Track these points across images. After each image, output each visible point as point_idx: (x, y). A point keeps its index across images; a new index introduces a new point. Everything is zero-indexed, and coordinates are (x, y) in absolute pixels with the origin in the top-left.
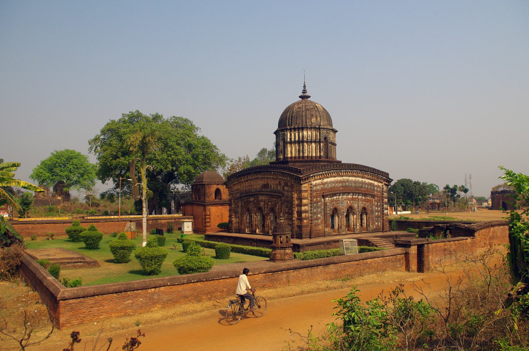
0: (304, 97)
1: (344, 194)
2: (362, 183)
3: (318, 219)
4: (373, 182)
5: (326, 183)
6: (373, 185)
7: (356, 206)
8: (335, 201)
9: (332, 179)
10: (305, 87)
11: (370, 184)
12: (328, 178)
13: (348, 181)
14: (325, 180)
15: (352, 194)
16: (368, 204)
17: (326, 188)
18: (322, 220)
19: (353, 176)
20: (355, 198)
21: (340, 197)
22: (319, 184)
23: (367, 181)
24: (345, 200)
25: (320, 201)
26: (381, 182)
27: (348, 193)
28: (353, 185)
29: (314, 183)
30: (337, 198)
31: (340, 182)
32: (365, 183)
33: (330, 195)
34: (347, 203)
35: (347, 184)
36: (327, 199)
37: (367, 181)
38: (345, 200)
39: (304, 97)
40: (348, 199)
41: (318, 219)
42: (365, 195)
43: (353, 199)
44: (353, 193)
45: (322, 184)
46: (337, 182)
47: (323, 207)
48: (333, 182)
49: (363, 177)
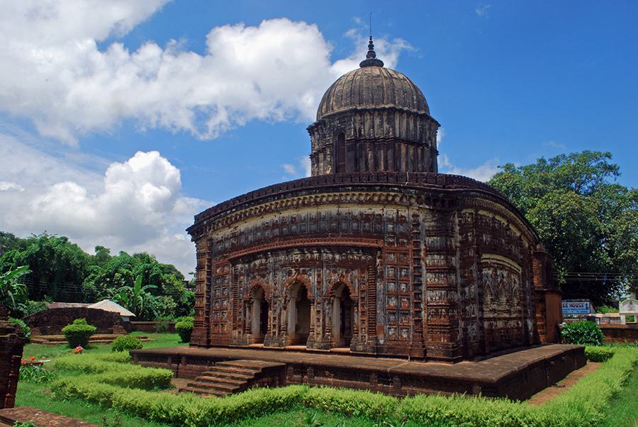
3: (222, 310)
4: (377, 210)
5: (242, 233)
6: (379, 219)
8: (258, 270)
9: (257, 222)
11: (367, 218)
13: (293, 220)
14: (242, 227)
18: (230, 313)
19: (309, 205)
20: (312, 259)
22: (227, 239)
23: (356, 210)
29: (219, 236)
30: (261, 264)
35: (294, 227)
36: (239, 266)
41: (222, 310)
43: (304, 263)
45: (234, 236)
46: (266, 227)
48: (257, 229)
49: (338, 203)
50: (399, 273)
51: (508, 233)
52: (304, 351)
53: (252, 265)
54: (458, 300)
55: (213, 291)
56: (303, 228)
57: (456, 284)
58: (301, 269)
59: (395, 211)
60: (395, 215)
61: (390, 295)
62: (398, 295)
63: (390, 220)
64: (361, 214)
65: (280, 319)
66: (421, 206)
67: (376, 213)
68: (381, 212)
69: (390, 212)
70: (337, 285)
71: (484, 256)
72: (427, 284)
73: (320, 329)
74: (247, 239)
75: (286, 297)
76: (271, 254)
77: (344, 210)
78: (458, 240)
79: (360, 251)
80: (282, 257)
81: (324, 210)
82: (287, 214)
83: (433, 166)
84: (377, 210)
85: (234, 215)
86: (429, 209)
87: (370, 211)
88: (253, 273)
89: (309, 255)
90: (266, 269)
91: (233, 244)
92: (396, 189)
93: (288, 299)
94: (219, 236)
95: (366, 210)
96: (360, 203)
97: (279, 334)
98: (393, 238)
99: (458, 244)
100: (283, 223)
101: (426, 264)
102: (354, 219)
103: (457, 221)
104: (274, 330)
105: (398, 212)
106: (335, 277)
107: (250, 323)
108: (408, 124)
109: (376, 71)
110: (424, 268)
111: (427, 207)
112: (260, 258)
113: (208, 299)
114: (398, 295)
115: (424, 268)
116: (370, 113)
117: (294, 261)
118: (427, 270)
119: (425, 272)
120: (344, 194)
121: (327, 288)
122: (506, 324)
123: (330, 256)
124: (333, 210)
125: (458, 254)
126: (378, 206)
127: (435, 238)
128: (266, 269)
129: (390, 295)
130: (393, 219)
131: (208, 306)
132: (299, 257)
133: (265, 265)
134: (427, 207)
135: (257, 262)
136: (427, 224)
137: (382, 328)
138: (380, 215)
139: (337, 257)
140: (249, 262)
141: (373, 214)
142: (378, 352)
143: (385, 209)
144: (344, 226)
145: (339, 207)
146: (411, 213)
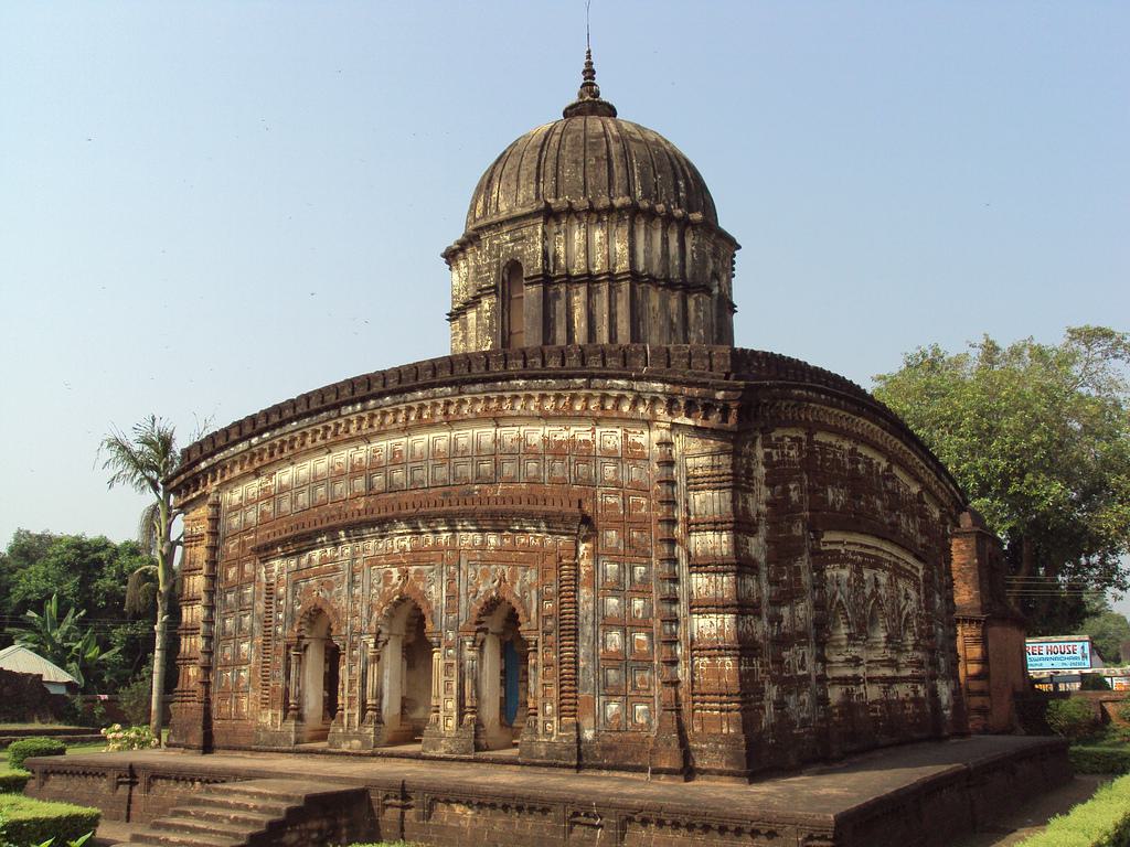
0: (590, 105)
1: (356, 528)
2: (497, 452)
3: (238, 662)
4: (581, 433)
5: (283, 489)
6: (586, 453)
7: (437, 593)
9: (320, 464)
10: (589, 72)
11: (557, 451)
12: (291, 461)
13: (396, 459)
14: (286, 475)
15: (402, 527)
16: (531, 576)
17: (281, 516)
18: (254, 671)
20: (436, 547)
21: (347, 549)
23: (536, 434)
24: (373, 561)
25: (252, 580)
26: (649, 423)
27: (382, 525)
28: (442, 473)
30: (324, 560)
31: (355, 471)
32: (524, 451)
33: (283, 543)
34: (387, 577)
36: (276, 564)
37: (536, 434)
38: (373, 561)
39: (590, 105)
40: (391, 558)
41: (238, 662)
42: (496, 520)
43: (417, 555)
44: (409, 520)
45: (268, 496)
46: (337, 475)
47: (260, 606)
48: (316, 480)
49: (497, 420)
50: (628, 575)
51: (890, 485)
52: (417, 757)
53: (304, 560)
54: (764, 637)
55: (218, 622)
56: (418, 474)
57: (759, 599)
58: (413, 569)
59: (619, 432)
60: (619, 443)
61: (608, 624)
62: (627, 625)
63: (611, 455)
64: (546, 441)
65: (364, 686)
66: (676, 421)
67: (582, 437)
68: (589, 437)
69: (610, 437)
70: (491, 606)
71: (828, 537)
72: (691, 601)
73: (452, 705)
74: (294, 501)
75: (379, 632)
76: (347, 536)
77: (509, 433)
78: (763, 497)
79: (543, 525)
80: (372, 545)
81: (465, 436)
82: (383, 445)
83: (724, 332)
84: (581, 433)
85: (266, 446)
86: (696, 427)
87: (566, 434)
88: (307, 579)
89: (431, 538)
90: (336, 570)
91: (263, 513)
92: (620, 382)
93: (382, 637)
94: (234, 496)
95: (560, 433)
96: (545, 417)
97: (362, 720)
98: (616, 494)
99: (763, 508)
100: (374, 466)
101: (689, 554)
102: (529, 452)
103: (760, 453)
104: (350, 711)
105: (626, 436)
106: (486, 588)
107: (300, 696)
108: (665, 241)
109: (596, 124)
110: (683, 561)
111: (690, 422)
112: (322, 545)
113: (209, 638)
114: (627, 625)
115: (683, 561)
116: (579, 218)
117: (396, 551)
118: (690, 566)
119: (685, 571)
120: (507, 395)
121: (468, 610)
122: (886, 690)
123: (478, 537)
124: (486, 434)
125: (763, 530)
126: (584, 422)
127: (709, 493)
128: (336, 570)
129: (608, 624)
130: (616, 451)
131: (209, 652)
132: (407, 543)
133: (334, 559)
134: (690, 422)
135: (316, 554)
136: (690, 462)
137: (590, 703)
138: (586, 442)
139: (493, 539)
140: (300, 553)
141: (572, 442)
142: (580, 759)
143: (598, 431)
144: (508, 469)
145: (498, 426)
146: (656, 435)
